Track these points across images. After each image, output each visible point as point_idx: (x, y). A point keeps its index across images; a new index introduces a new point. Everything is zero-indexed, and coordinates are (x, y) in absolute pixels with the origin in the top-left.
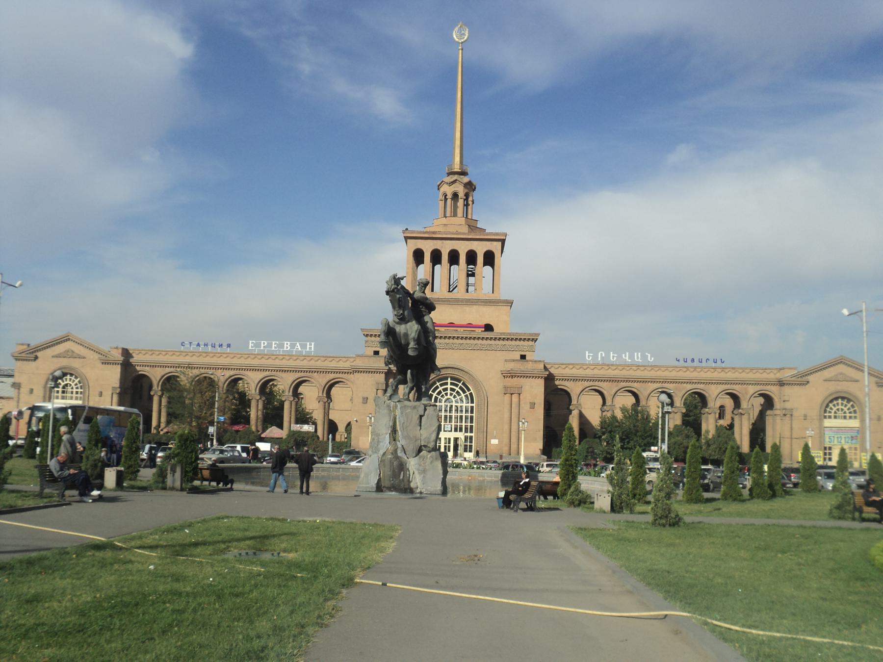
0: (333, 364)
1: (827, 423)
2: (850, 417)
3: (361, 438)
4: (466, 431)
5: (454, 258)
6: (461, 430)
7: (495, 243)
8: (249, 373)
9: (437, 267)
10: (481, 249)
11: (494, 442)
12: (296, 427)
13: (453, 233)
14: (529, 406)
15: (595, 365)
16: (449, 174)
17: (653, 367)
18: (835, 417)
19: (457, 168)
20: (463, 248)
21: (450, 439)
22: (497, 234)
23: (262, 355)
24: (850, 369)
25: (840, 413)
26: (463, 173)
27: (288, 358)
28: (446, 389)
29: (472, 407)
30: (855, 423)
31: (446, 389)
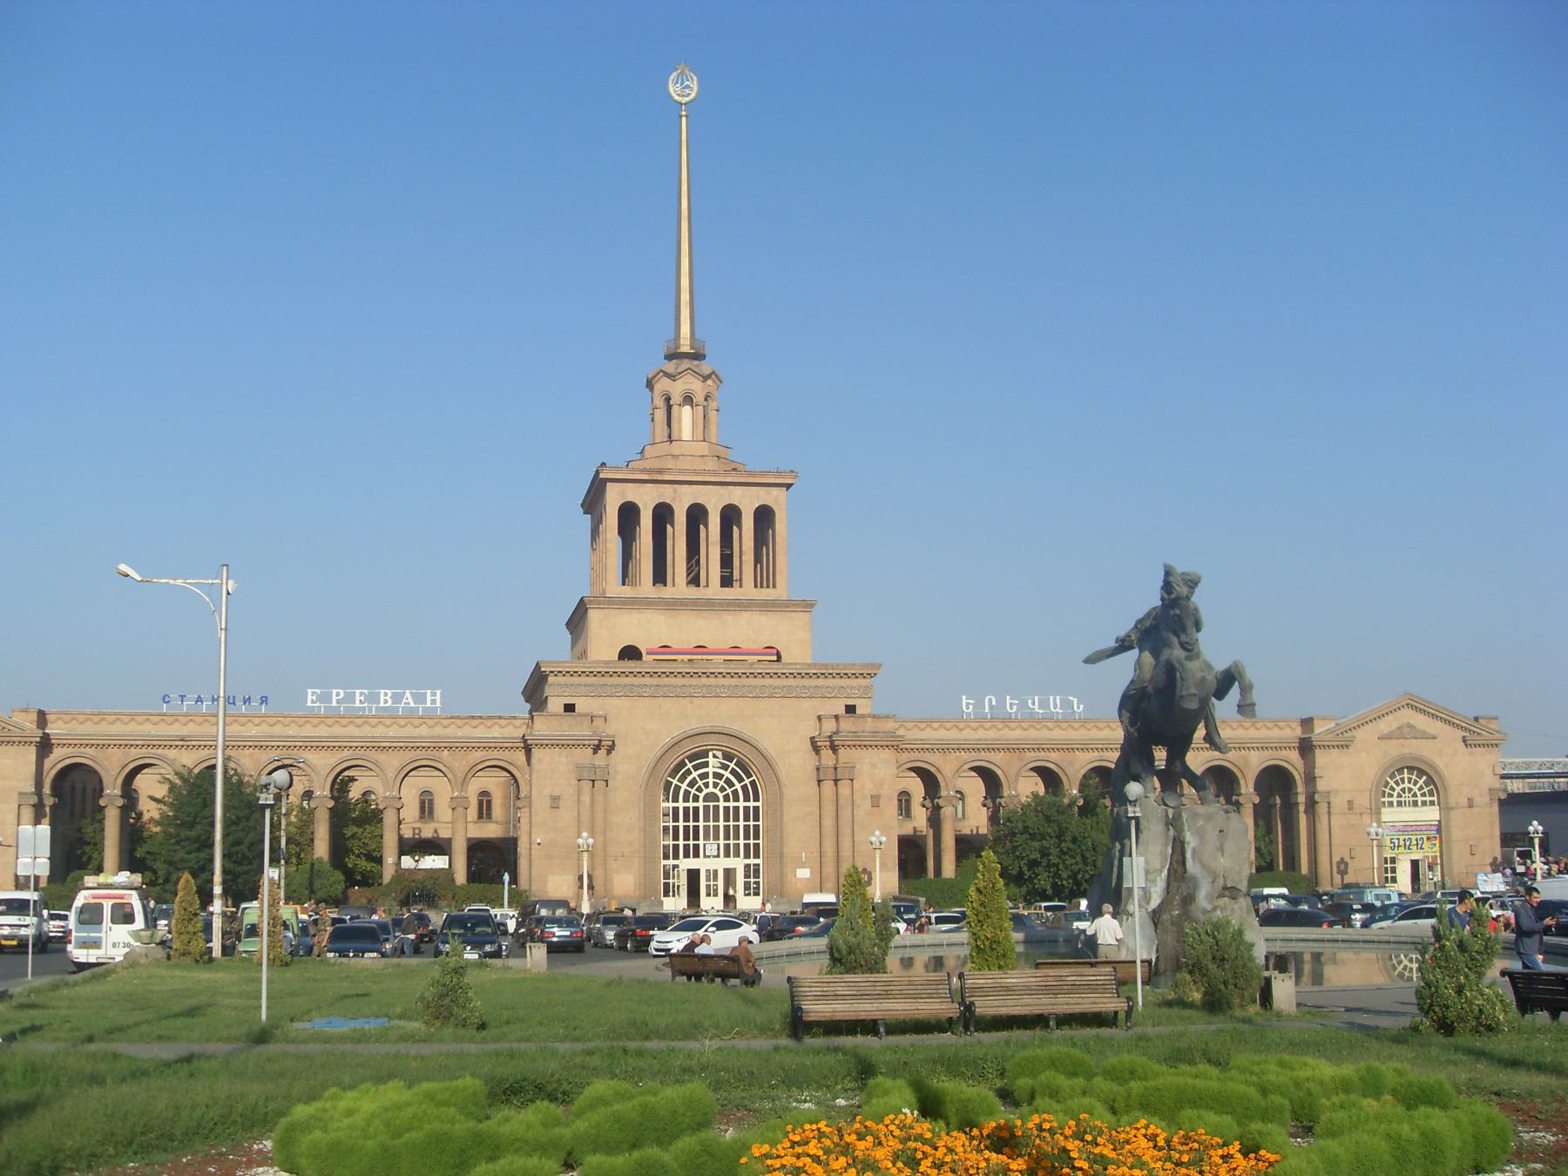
0: (481, 732)
1: (1388, 815)
2: (1424, 803)
3: (550, 878)
4: (747, 856)
6: (737, 855)
7: (775, 491)
8: (311, 757)
10: (748, 502)
12: (407, 862)
13: (695, 472)
14: (868, 802)
15: (981, 720)
16: (673, 356)
17: (1084, 722)
18: (1399, 804)
19: (685, 347)
20: (714, 501)
21: (716, 872)
22: (779, 473)
23: (334, 717)
24: (1421, 717)
25: (1407, 797)
26: (698, 356)
27: (388, 722)
28: (705, 776)
29: (756, 809)
30: (1431, 814)
31: (705, 776)
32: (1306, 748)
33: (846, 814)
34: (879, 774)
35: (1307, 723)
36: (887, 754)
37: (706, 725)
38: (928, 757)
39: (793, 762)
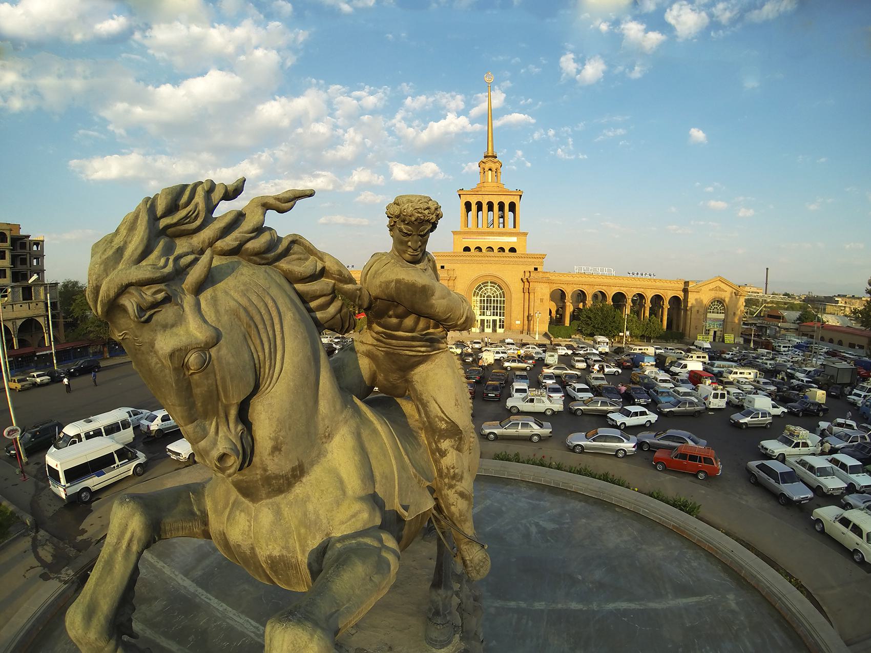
1: (709, 315)
5: (490, 206)
9: (480, 213)
11: (518, 322)
20: (496, 201)
30: (722, 316)
32: (686, 291)
33: (532, 304)
34: (543, 291)
35: (687, 283)
36: (546, 285)
37: (487, 273)
38: (563, 286)
39: (516, 287)
